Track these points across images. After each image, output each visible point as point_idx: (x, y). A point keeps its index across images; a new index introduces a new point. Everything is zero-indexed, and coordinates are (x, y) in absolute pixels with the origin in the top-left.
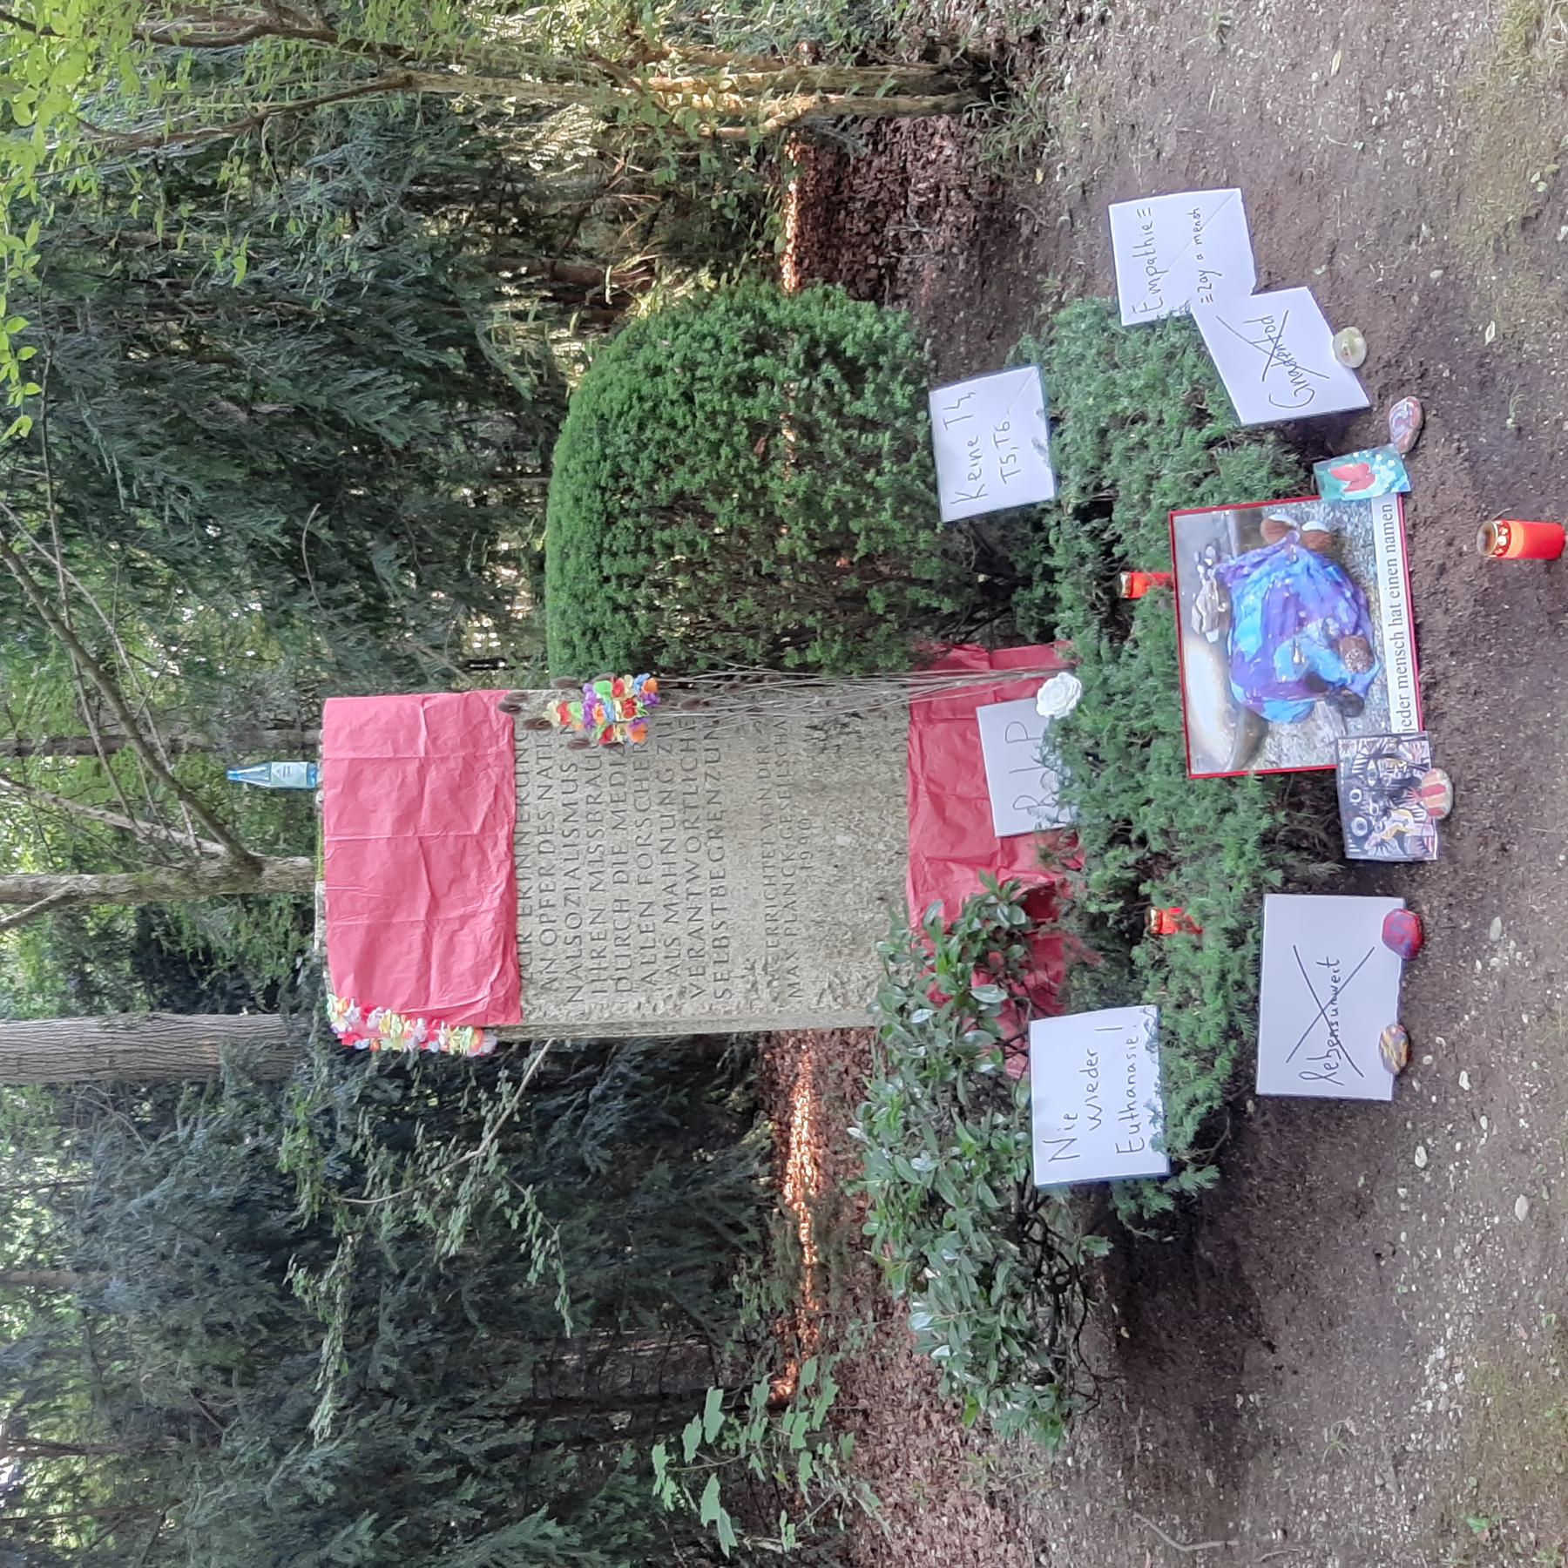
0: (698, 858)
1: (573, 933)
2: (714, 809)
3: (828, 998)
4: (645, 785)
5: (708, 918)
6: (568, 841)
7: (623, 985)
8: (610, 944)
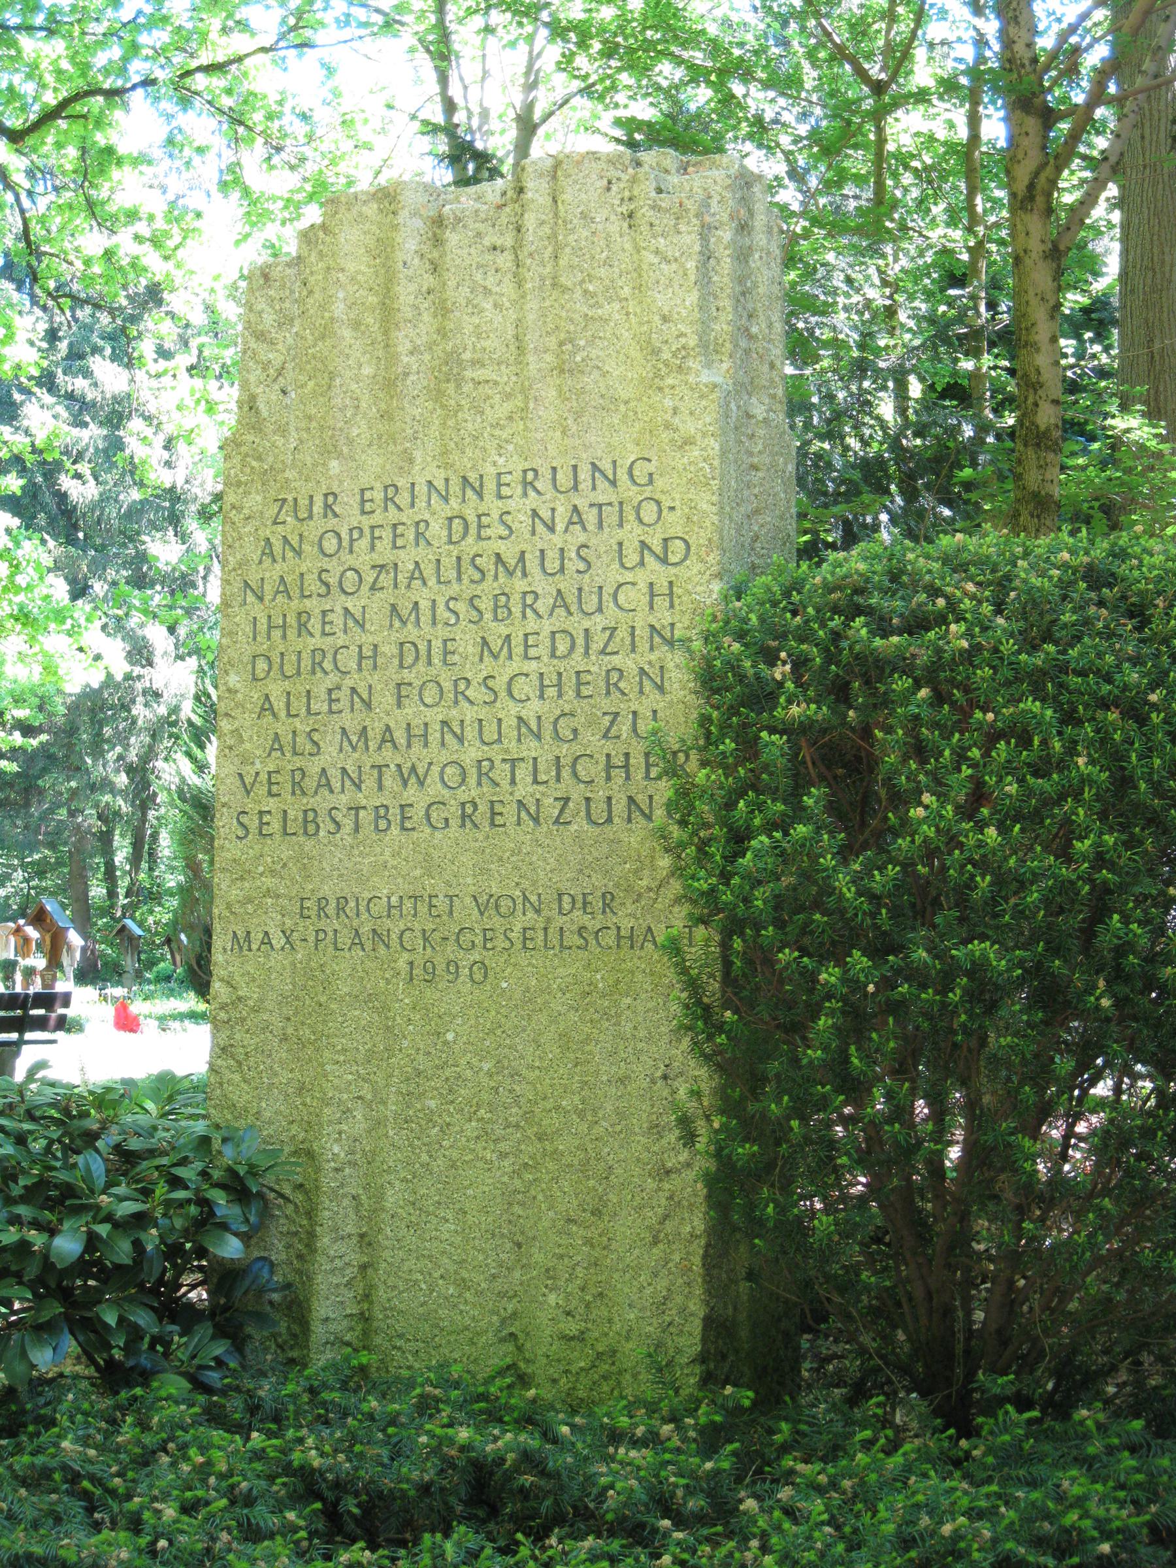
0: (435, 788)
2: (509, 812)
4: (551, 692)
6: (465, 563)
7: (262, 665)
8: (316, 641)
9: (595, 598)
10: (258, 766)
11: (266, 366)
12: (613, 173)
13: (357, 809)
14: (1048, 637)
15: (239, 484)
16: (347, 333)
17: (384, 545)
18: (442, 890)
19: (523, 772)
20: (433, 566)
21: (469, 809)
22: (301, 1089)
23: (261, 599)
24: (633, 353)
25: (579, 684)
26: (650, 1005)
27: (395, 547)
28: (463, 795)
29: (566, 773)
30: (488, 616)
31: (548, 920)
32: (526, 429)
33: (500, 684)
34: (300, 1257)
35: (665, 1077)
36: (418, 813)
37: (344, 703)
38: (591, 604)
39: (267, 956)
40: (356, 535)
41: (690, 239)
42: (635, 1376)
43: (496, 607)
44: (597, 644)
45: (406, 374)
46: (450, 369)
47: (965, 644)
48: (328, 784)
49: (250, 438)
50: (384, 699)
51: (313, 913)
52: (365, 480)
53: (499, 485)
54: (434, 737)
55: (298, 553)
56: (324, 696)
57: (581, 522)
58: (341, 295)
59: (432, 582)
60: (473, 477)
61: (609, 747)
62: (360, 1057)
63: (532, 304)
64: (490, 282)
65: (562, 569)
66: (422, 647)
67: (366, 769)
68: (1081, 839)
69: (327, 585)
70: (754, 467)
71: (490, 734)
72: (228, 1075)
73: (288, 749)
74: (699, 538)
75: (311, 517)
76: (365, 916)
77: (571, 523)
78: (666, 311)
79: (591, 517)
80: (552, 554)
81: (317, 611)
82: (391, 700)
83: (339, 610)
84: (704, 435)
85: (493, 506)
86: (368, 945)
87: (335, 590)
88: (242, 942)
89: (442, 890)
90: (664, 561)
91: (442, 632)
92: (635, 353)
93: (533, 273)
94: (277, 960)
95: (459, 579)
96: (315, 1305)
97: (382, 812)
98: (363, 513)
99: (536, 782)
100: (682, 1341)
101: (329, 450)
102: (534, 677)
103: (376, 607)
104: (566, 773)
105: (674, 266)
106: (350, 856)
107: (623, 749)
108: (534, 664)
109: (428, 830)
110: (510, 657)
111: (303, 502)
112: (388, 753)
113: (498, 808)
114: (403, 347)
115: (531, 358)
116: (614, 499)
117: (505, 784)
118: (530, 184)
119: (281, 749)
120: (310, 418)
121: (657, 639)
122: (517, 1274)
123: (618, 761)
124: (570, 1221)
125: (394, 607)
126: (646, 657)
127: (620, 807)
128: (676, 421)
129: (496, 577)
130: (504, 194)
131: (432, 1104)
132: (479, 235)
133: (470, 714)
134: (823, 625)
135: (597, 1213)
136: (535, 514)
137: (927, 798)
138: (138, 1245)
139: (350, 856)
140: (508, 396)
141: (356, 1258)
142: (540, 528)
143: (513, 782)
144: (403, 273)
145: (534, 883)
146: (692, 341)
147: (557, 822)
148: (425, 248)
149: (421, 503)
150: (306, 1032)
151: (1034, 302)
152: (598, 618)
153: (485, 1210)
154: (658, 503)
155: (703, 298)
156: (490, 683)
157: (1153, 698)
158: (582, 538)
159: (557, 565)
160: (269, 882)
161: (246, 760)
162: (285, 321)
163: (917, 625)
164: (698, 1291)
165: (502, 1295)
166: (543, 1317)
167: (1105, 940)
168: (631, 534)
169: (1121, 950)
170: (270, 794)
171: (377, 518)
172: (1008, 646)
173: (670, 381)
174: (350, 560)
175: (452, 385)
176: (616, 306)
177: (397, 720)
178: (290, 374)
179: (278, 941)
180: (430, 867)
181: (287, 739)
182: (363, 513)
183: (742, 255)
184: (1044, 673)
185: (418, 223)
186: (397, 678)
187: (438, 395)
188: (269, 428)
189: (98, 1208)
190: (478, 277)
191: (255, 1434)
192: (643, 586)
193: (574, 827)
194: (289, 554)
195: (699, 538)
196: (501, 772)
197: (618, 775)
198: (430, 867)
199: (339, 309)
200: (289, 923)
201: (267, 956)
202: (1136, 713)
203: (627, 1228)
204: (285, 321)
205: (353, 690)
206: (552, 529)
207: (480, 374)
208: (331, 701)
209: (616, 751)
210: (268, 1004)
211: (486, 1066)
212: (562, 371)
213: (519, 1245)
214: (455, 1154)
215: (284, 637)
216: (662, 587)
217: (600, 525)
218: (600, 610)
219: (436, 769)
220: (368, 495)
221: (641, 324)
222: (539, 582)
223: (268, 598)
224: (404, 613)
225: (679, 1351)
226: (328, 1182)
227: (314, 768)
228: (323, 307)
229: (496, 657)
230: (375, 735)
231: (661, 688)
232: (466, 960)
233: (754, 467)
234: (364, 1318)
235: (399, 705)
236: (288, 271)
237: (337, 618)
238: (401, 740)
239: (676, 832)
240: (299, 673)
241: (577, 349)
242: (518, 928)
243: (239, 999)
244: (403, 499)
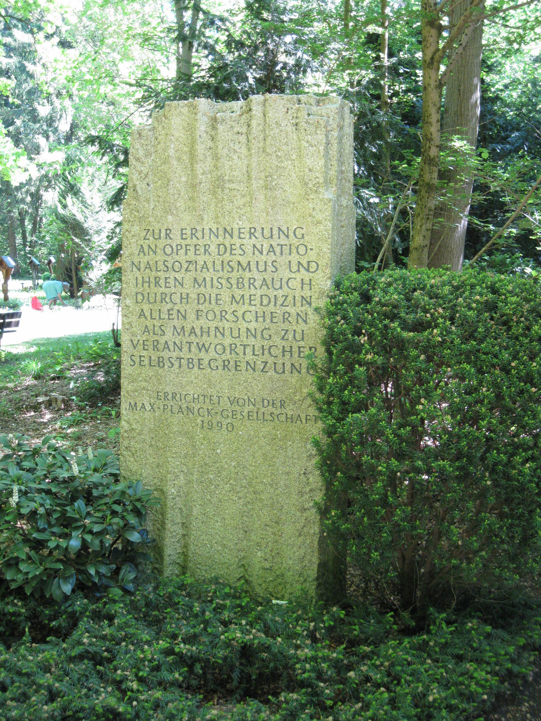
0: (212, 354)
2: (243, 366)
4: (261, 319)
5: (175, 354)
6: (225, 264)
7: (140, 297)
8: (163, 290)
9: (279, 283)
10: (139, 337)
11: (140, 173)
12: (289, 105)
13: (180, 359)
14: (471, 336)
15: (129, 221)
16: (175, 162)
17: (191, 253)
18: (215, 394)
19: (249, 350)
20: (212, 263)
21: (226, 363)
22: (158, 466)
23: (139, 270)
24: (296, 183)
25: (272, 317)
26: (299, 445)
27: (196, 254)
28: (224, 357)
29: (266, 352)
30: (235, 286)
31: (258, 409)
32: (251, 211)
33: (239, 314)
34: (158, 529)
35: (305, 474)
36: (205, 362)
37: (175, 316)
39: (144, 413)
41: (321, 137)
42: (292, 585)
43: (238, 283)
44: (280, 301)
45: (201, 183)
46: (219, 183)
47: (440, 339)
48: (168, 348)
49: (134, 202)
50: (192, 316)
51: (162, 398)
52: (183, 226)
53: (240, 233)
54: (212, 333)
55: (155, 253)
56: (166, 312)
57: (274, 251)
58: (172, 146)
59: (211, 270)
60: (228, 228)
61: (284, 343)
62: (182, 455)
63: (255, 159)
64: (237, 147)
65: (265, 270)
66: (207, 296)
67: (184, 343)
68: (483, 420)
69: (167, 267)
70: (342, 227)
71: (235, 333)
72: (128, 458)
73: (151, 332)
74: (323, 262)
75: (160, 238)
76: (183, 401)
77: (269, 251)
78: (311, 167)
79: (278, 250)
80: (261, 264)
81: (163, 277)
82: (195, 317)
84: (326, 220)
85: (238, 242)
86: (185, 413)
87: (170, 269)
88: (133, 407)
89: (215, 394)
90: (308, 270)
91: (216, 291)
92: (297, 183)
93: (256, 145)
94: (147, 415)
95: (223, 270)
96: (165, 550)
98: (182, 239)
99: (254, 354)
100: (310, 573)
101: (168, 211)
102: (254, 313)
103: (188, 278)
104: (266, 352)
105: (315, 148)
106: (177, 377)
107: (290, 344)
108: (254, 307)
109: (210, 370)
110: (244, 304)
111: (157, 232)
112: (193, 337)
113: (238, 364)
114: (199, 171)
115: (254, 182)
116: (287, 243)
117: (241, 354)
118: (254, 108)
119: (148, 331)
120: (159, 197)
121: (304, 302)
122: (245, 542)
123: (288, 349)
124: (266, 525)
125: (195, 279)
126: (299, 309)
127: (288, 367)
128: (314, 213)
129: (238, 271)
130: (242, 108)
131: (212, 476)
132: (232, 127)
133: (227, 325)
134: (381, 322)
135: (277, 523)
136: (254, 246)
137: (423, 400)
138: (101, 542)
139: (177, 377)
140: (244, 196)
141: (181, 531)
142: (256, 252)
143: (244, 354)
144: (199, 140)
145: (253, 394)
146: (321, 180)
147: (262, 371)
148: (209, 129)
149: (207, 237)
150: (160, 444)
151: (431, 105)
152: (280, 291)
153: (233, 519)
154: (306, 246)
155: (326, 162)
156: (235, 313)
157: (513, 364)
158: (274, 258)
159: (263, 268)
160: (144, 384)
161: (134, 334)
162: (148, 154)
163: (419, 326)
164: (316, 554)
165: (239, 550)
166: (256, 561)
167: (490, 461)
168: (294, 258)
169: (496, 464)
170: (144, 349)
171: (188, 241)
172: (457, 341)
173: (312, 197)
174: (177, 258)
175: (220, 190)
176: (290, 162)
177: (197, 325)
178: (150, 177)
179: (148, 407)
180: (210, 385)
181: (151, 328)
182: (182, 239)
183: (340, 142)
184: (471, 352)
185: (205, 119)
186: (197, 308)
187: (215, 193)
188: (142, 200)
189: (84, 526)
190: (232, 145)
191: (161, 642)
192: (299, 280)
193: (269, 374)
194: (151, 253)
195: (323, 262)
196: (240, 350)
197: (288, 355)
198: (210, 385)
199: (171, 152)
200: (152, 401)
201: (144, 413)
202: (506, 369)
203: (289, 529)
204: (148, 154)
205: (178, 311)
206: (261, 253)
207: (232, 186)
208: (169, 314)
210: (145, 432)
211: (233, 464)
212: (266, 188)
213: (246, 532)
214: (221, 497)
215: (149, 286)
216: (307, 281)
217: (282, 253)
218: (281, 288)
219: (213, 346)
220: (184, 232)
221: (300, 172)
222: (255, 274)
223: (142, 269)
224: (200, 282)
225: (308, 576)
226: (170, 503)
227: (162, 340)
228: (164, 150)
229: (238, 303)
230: (188, 329)
231: (305, 322)
232: (225, 422)
233: (342, 227)
234: (185, 555)
235: (198, 319)
236: (149, 133)
237: (171, 281)
238: (199, 333)
239: (318, 395)
240: (155, 302)
241: (273, 179)
242: (246, 411)
244: (199, 235)
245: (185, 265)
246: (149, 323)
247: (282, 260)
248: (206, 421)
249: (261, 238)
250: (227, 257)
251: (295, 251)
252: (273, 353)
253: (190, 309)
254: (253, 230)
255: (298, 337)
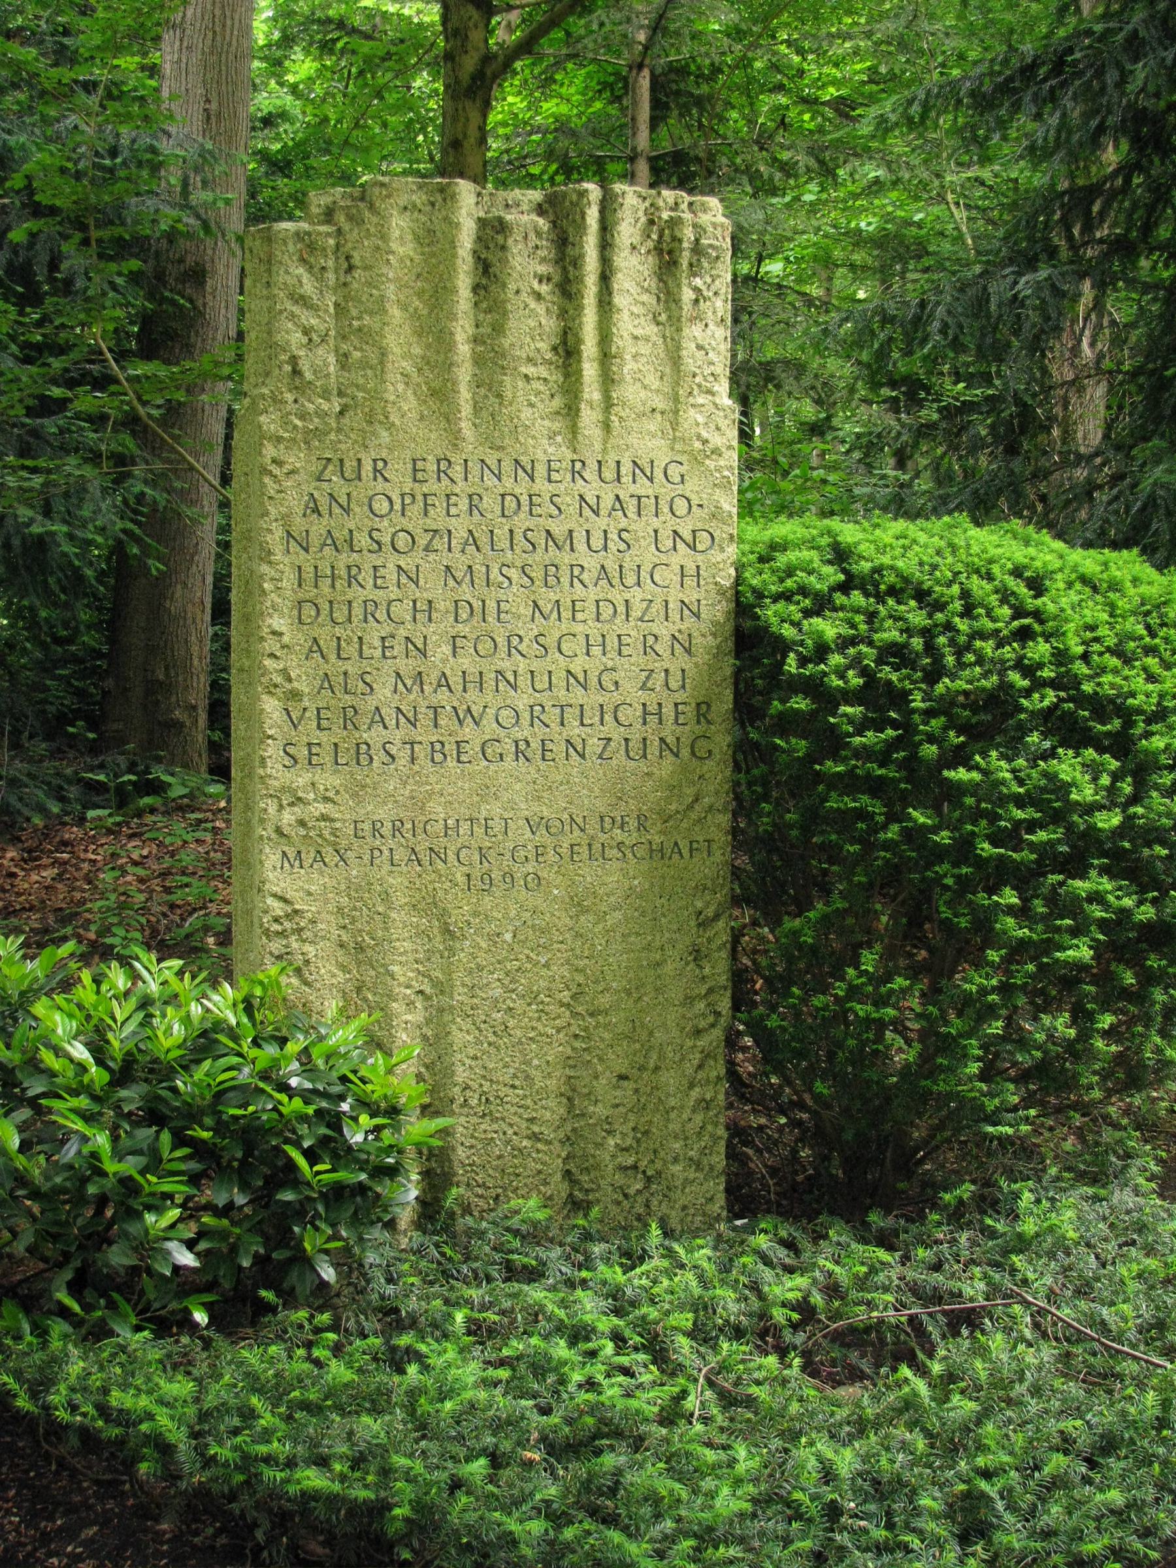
0: (489, 727)
1: (386, 539)
2: (559, 748)
3: (278, 908)
4: (596, 651)
6: (518, 537)
7: (309, 611)
19: (571, 715)
33: (550, 641)
37: (398, 650)
38: (630, 580)
39: (321, 873)
40: (408, 501)
44: (636, 613)
55: (347, 510)
60: (524, 460)
65: (605, 548)
66: (477, 604)
82: (447, 649)
83: (391, 566)
86: (426, 861)
90: (694, 549)
97: (438, 747)
112: (443, 696)
116: (650, 492)
123: (653, 708)
133: (522, 665)
142: (587, 512)
156: (541, 640)
158: (624, 523)
174: (404, 523)
193: (614, 762)
194: (337, 510)
206: (596, 513)
209: (651, 700)
216: (691, 569)
243: (296, 912)
244: (457, 471)
245: (422, 541)
246: (335, 666)
247: (641, 528)
248: (476, 873)
249: (597, 483)
250: (522, 521)
251: (666, 510)
252: (622, 719)
253: (437, 632)
254: (578, 465)
255: (674, 685)
